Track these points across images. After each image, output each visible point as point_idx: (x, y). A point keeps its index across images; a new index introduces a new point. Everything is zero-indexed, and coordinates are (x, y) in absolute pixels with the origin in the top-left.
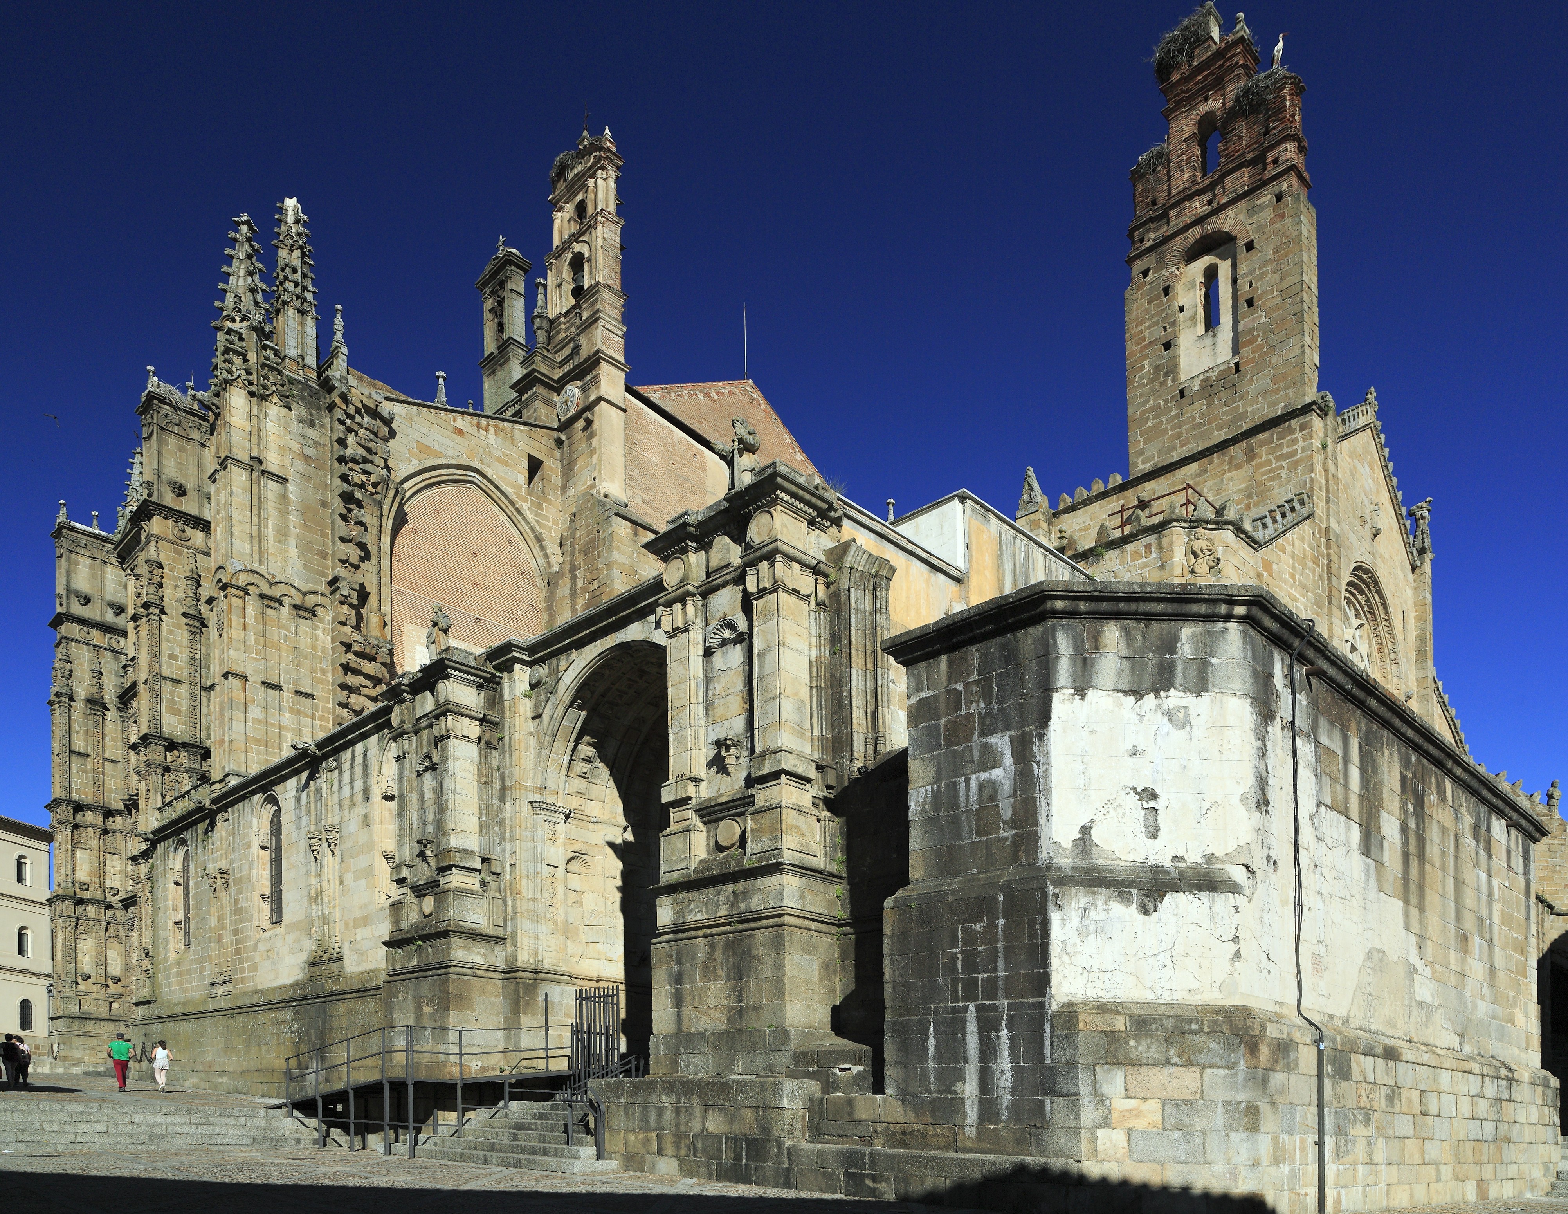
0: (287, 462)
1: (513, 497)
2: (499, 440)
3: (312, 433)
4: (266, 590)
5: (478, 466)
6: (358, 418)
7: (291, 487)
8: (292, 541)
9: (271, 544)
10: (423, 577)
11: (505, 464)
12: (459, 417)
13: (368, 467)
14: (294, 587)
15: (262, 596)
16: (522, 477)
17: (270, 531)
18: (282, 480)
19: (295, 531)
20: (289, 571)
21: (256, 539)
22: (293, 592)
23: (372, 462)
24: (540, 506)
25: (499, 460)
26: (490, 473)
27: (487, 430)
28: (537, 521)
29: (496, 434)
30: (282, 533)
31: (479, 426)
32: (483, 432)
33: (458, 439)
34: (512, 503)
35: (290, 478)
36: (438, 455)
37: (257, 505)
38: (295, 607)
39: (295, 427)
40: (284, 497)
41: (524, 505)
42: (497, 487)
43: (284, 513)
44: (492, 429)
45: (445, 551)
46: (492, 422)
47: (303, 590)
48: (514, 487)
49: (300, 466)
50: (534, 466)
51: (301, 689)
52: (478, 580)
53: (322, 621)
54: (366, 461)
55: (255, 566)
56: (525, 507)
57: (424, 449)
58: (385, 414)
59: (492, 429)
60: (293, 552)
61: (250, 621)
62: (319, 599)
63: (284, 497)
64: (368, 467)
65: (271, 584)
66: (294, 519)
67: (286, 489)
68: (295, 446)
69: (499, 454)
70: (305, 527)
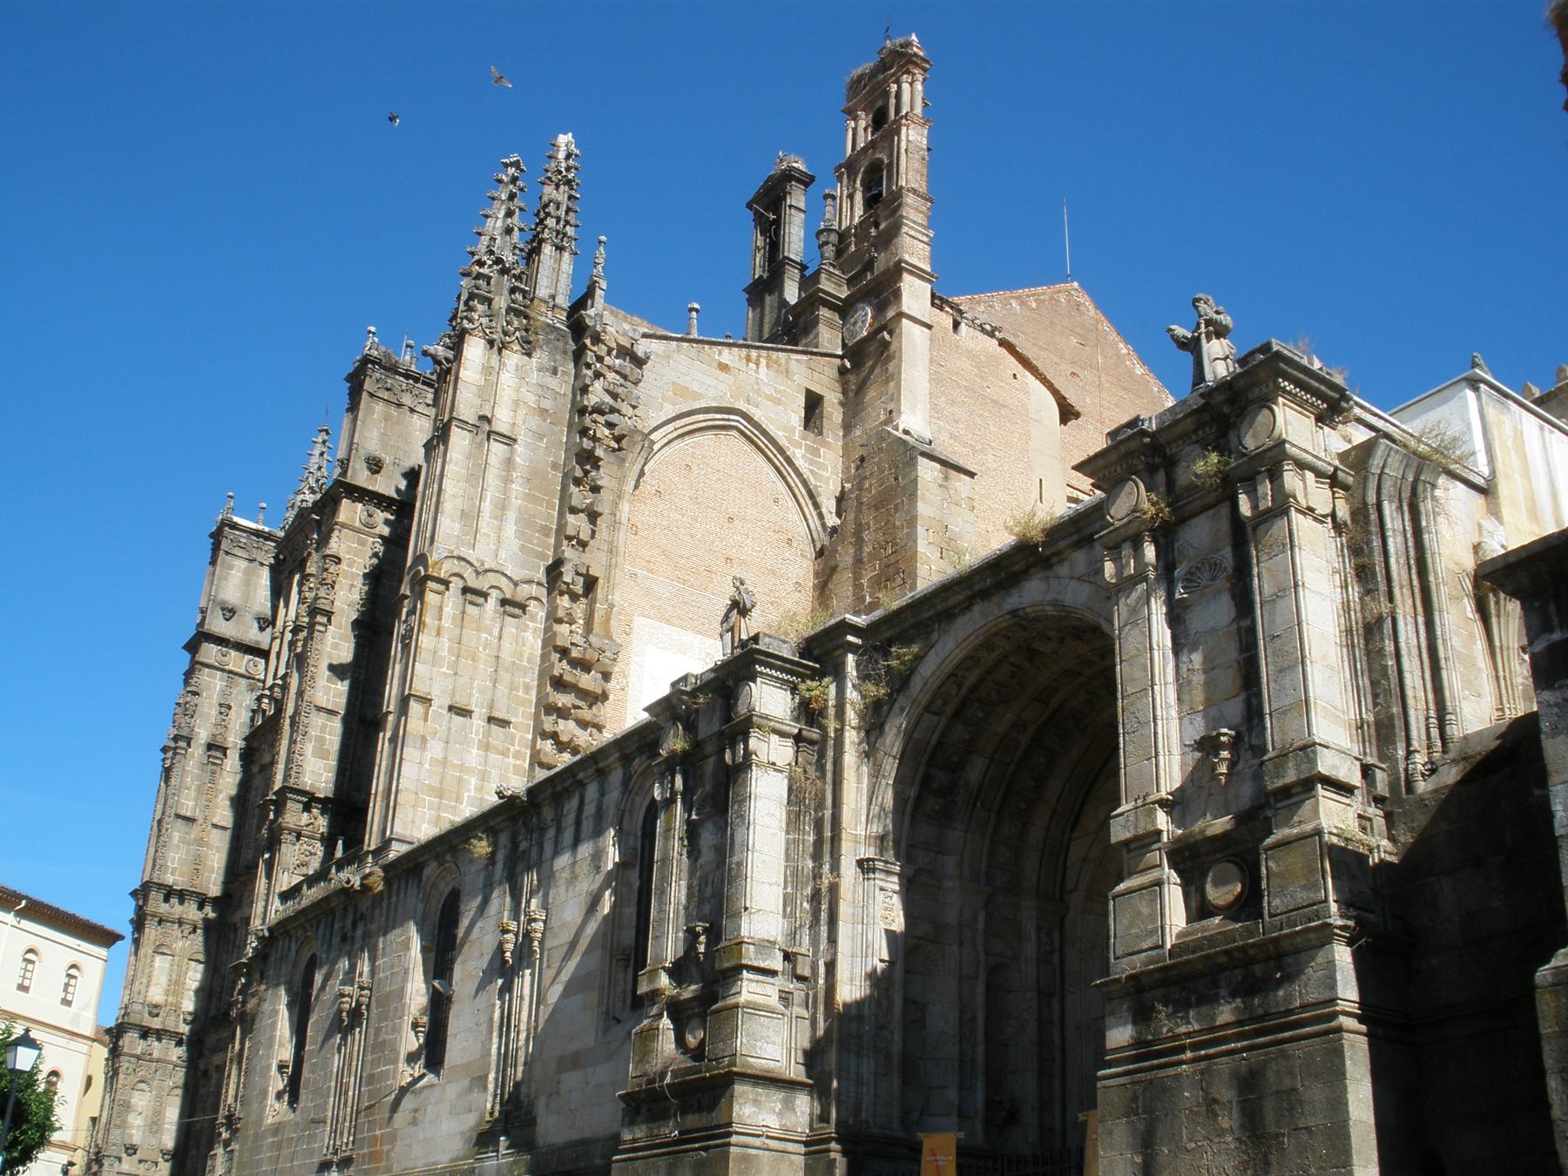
0: (519, 421)
1: (783, 442)
2: (772, 374)
3: (553, 382)
4: (473, 582)
5: (744, 407)
6: (607, 360)
7: (518, 448)
8: (511, 516)
9: (486, 523)
10: (664, 553)
11: (777, 402)
12: (726, 351)
13: (613, 418)
14: (506, 575)
15: (466, 590)
16: (796, 416)
17: (487, 506)
18: (510, 440)
19: (516, 502)
20: (503, 554)
21: (470, 517)
22: (504, 583)
23: (619, 412)
24: (816, 453)
25: (769, 398)
26: (757, 414)
27: (757, 365)
28: (812, 472)
29: (768, 366)
30: (502, 506)
31: (748, 359)
32: (752, 366)
33: (723, 376)
34: (781, 451)
35: (520, 438)
36: (696, 396)
37: (477, 474)
38: (504, 602)
39: (534, 377)
40: (509, 463)
41: (797, 451)
42: (765, 433)
43: (507, 481)
44: (763, 362)
45: (694, 519)
46: (764, 353)
47: (516, 578)
48: (785, 429)
49: (534, 422)
50: (813, 403)
51: (496, 714)
52: (732, 553)
53: (533, 619)
54: (613, 410)
55: (465, 552)
56: (799, 456)
57: (681, 391)
58: (640, 354)
59: (763, 362)
60: (510, 529)
61: (446, 623)
62: (534, 590)
63: (509, 463)
64: (613, 418)
65: (477, 573)
66: (516, 487)
67: (512, 452)
68: (531, 400)
69: (768, 390)
70: (529, 498)
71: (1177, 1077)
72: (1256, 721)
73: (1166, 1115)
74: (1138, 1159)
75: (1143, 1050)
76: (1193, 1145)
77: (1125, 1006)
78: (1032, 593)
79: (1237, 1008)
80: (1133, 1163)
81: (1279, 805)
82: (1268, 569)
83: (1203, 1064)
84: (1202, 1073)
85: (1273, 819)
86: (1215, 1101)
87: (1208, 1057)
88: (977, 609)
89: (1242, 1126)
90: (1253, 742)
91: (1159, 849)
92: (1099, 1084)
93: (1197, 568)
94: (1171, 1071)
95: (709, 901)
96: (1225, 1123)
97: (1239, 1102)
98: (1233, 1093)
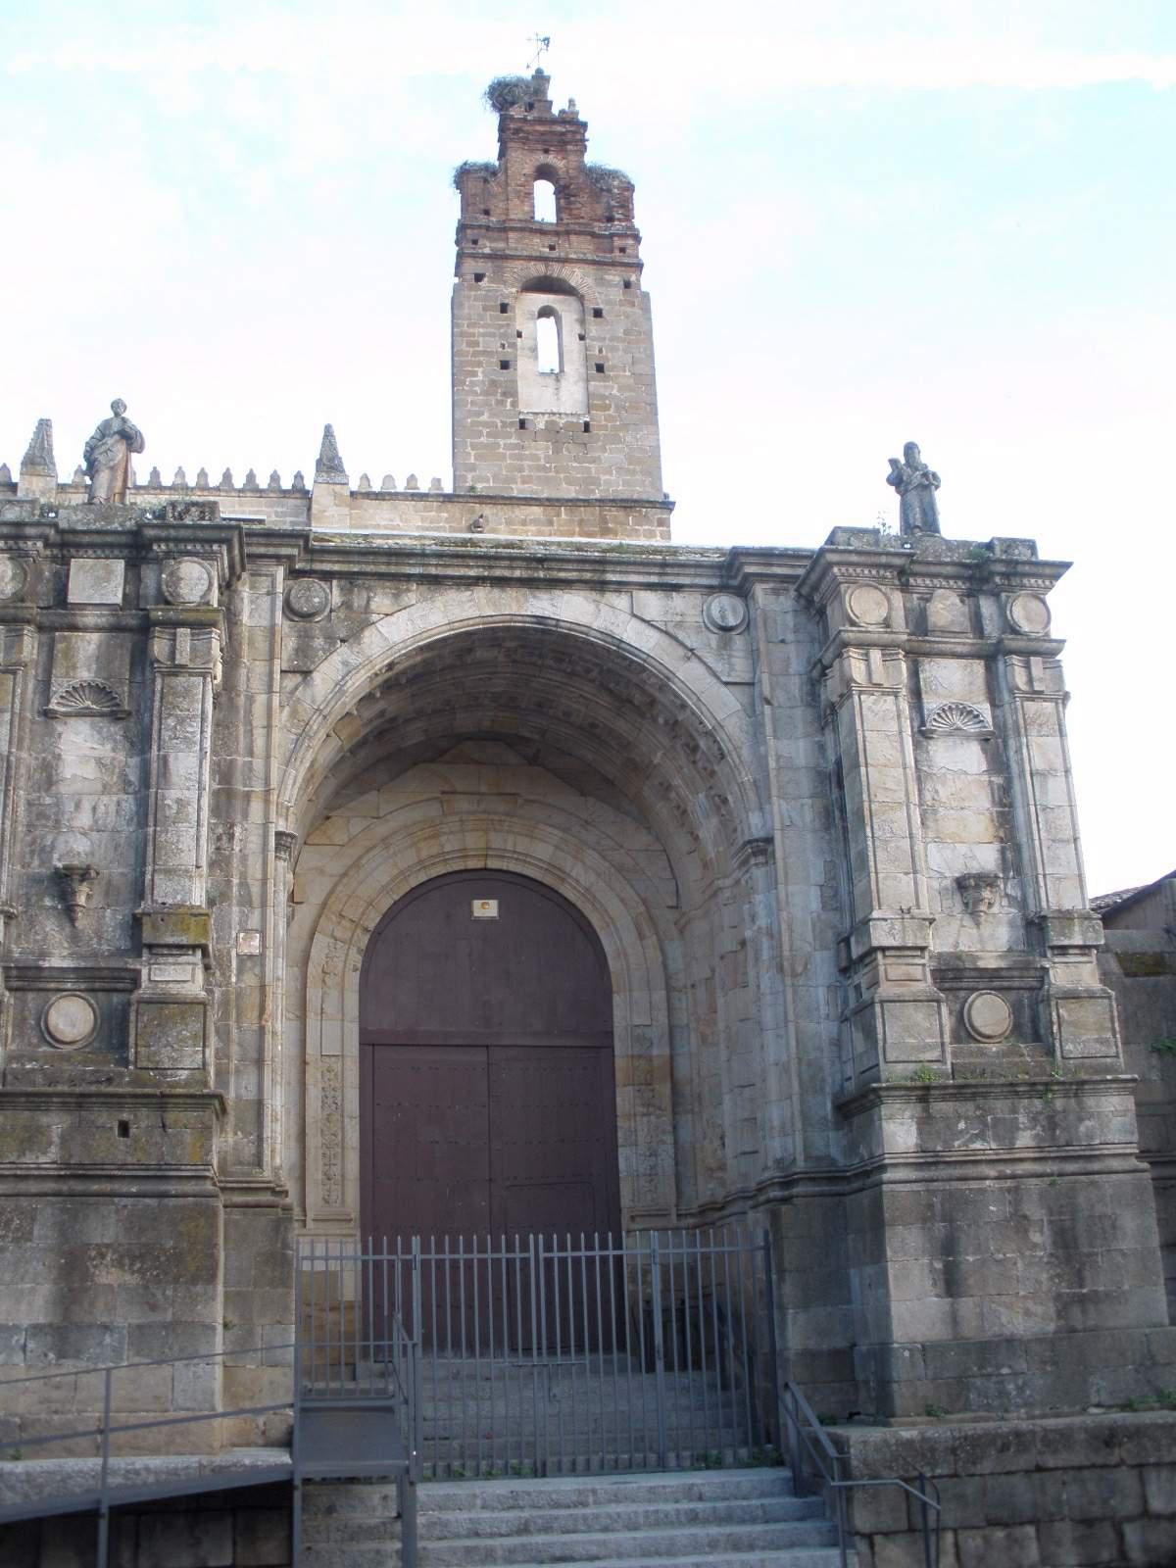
71: (982, 1191)
72: (1012, 873)
73: (969, 1226)
74: (938, 1265)
75: (928, 1160)
76: (1001, 1256)
77: (908, 1114)
78: (572, 609)
79: (1037, 1135)
80: (932, 1270)
81: (1056, 960)
82: (1039, 746)
83: (1009, 1183)
84: (1009, 1190)
85: (1051, 972)
86: (1025, 1217)
87: (1013, 1177)
88: (481, 593)
89: (1055, 1243)
90: (1009, 891)
91: (924, 965)
92: (885, 1187)
93: (950, 707)
94: (974, 1185)
95: (84, 834)
96: (1036, 1237)
97: (1050, 1222)
98: (1043, 1211)
